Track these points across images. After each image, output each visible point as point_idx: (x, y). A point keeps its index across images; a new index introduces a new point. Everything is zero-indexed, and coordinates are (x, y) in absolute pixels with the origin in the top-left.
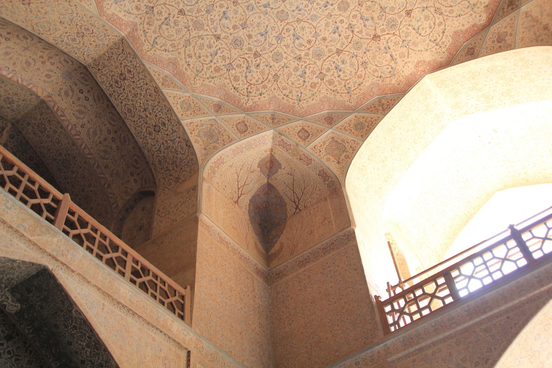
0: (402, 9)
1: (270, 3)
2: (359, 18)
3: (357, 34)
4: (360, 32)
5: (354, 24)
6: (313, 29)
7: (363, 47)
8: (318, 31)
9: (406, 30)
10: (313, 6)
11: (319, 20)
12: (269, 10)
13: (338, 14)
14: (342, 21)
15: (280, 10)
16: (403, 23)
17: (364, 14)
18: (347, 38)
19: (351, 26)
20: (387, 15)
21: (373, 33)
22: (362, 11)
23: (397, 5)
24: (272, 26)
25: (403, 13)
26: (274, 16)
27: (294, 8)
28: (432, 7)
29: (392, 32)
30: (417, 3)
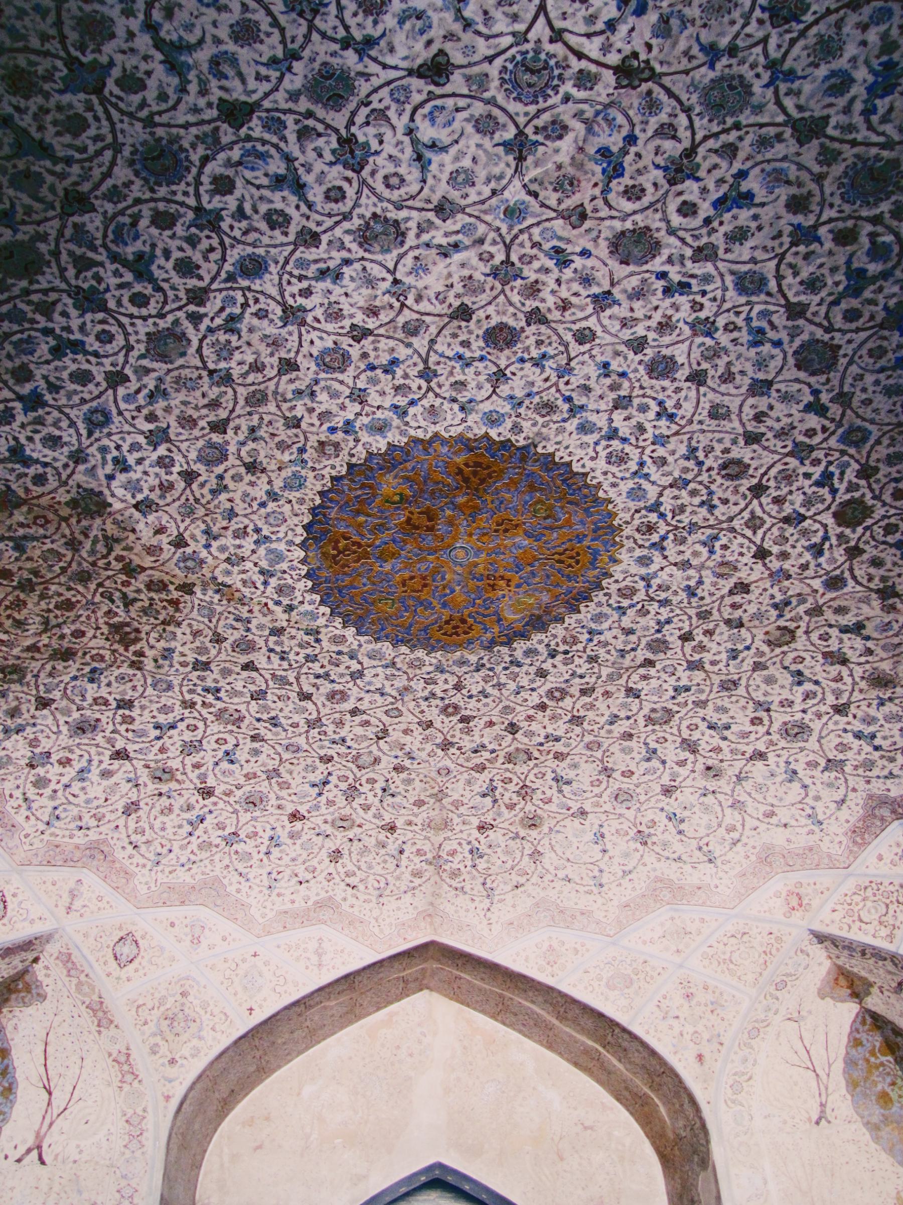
0: (450, 102)
1: (801, 407)
2: (626, 181)
3: (684, 134)
4: (667, 131)
5: (659, 173)
6: (789, 258)
7: (712, 75)
8: (786, 240)
9: (498, 14)
10: (716, 315)
11: (744, 268)
12: (825, 398)
13: (673, 240)
14: (688, 209)
15: (802, 375)
16: (483, 48)
17: (599, 176)
18: (730, 151)
19: (679, 170)
20: (521, 120)
21: (633, 99)
22: (597, 191)
23: (456, 125)
24: (872, 361)
25: (457, 82)
26: (835, 377)
27: (767, 348)
28: (324, 35)
29: (558, 49)
30: (375, 82)
